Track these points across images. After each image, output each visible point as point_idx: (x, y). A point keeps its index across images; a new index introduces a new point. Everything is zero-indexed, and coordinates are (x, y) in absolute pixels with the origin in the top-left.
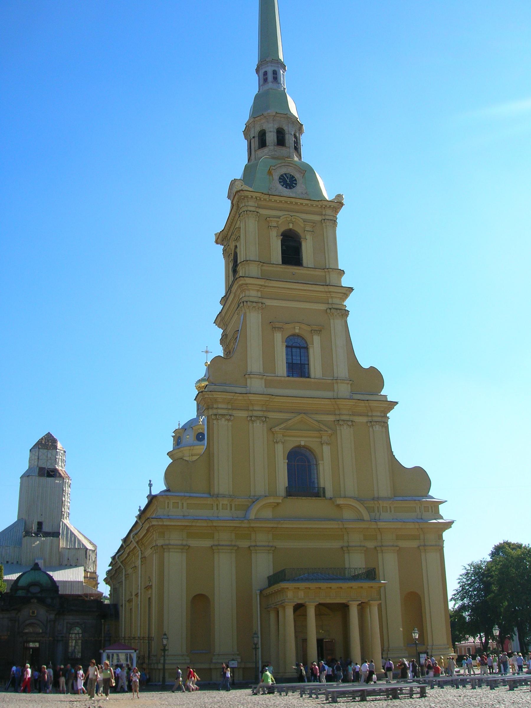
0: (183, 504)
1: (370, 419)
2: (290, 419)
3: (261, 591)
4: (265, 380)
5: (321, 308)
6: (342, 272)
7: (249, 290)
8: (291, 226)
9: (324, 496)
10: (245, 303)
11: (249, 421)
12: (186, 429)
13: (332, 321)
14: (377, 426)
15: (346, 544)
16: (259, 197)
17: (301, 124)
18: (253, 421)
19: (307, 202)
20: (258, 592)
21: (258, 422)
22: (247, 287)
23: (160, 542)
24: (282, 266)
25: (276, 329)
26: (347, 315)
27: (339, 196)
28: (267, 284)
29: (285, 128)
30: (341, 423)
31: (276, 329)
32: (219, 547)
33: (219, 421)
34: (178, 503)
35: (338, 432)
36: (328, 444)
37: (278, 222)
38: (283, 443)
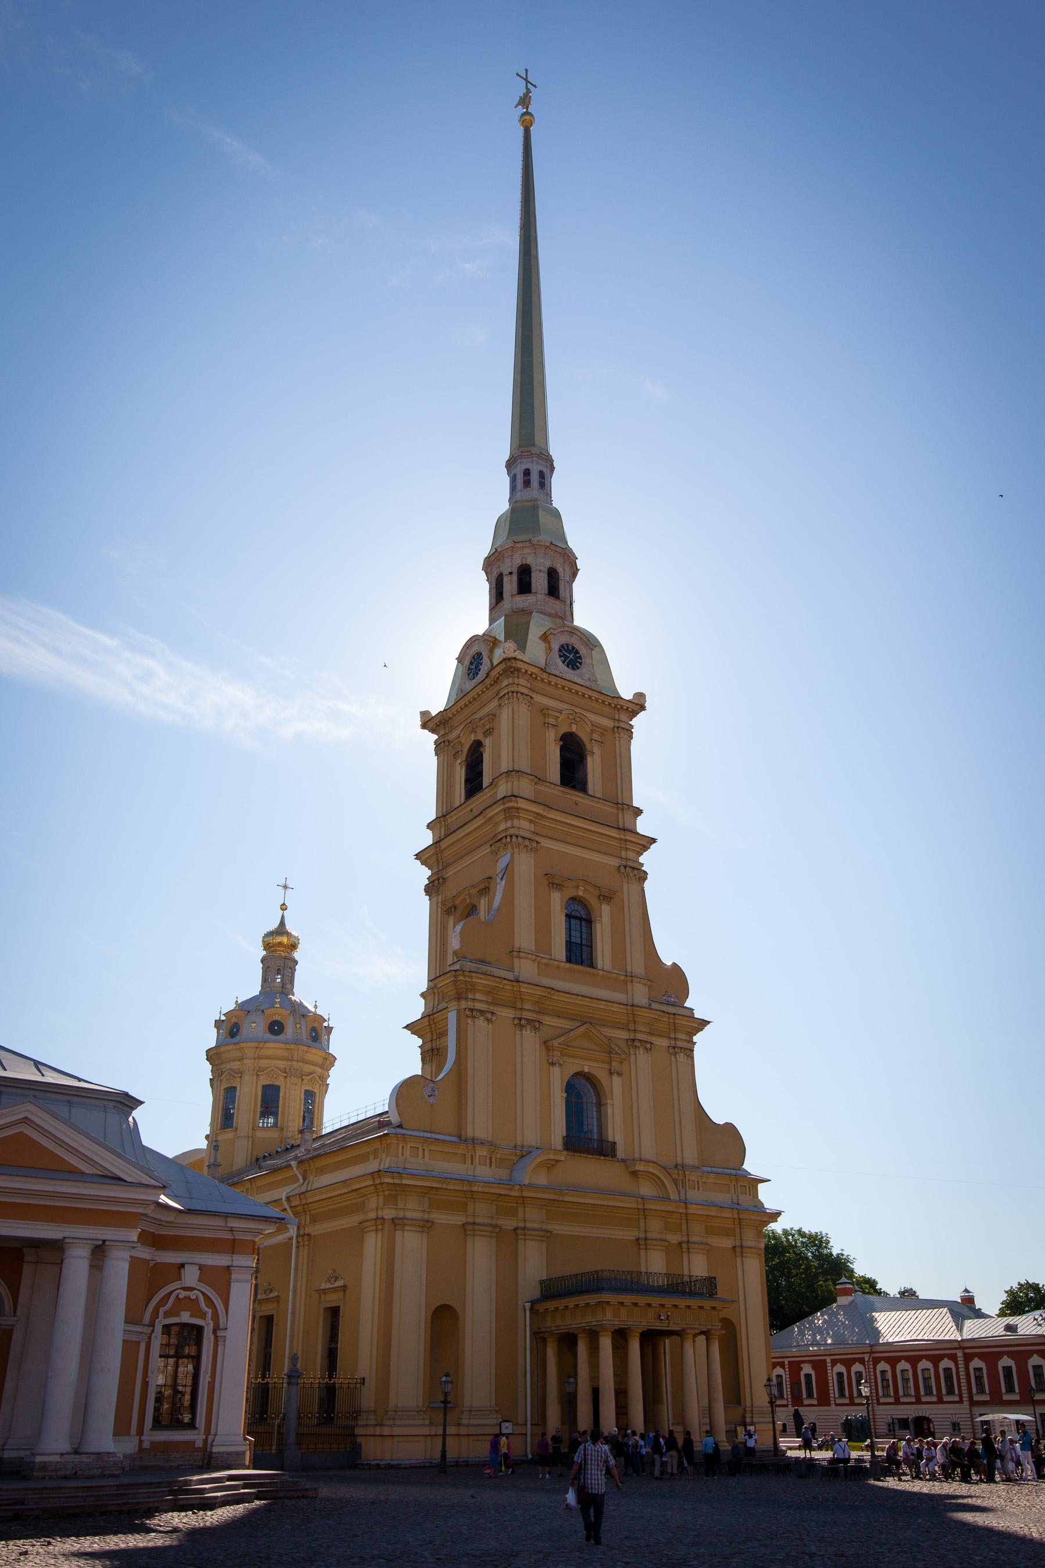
0: (424, 1149)
1: (673, 1042)
2: (572, 1030)
3: (532, 1308)
4: (539, 963)
5: (612, 863)
6: (638, 812)
7: (519, 818)
8: (574, 729)
9: (615, 1156)
10: (514, 838)
11: (515, 1025)
12: (249, 1012)
13: (625, 885)
14: (682, 1055)
15: (642, 1235)
16: (535, 674)
17: (577, 568)
18: (522, 1026)
19: (595, 695)
20: (528, 1305)
21: (528, 1027)
22: (518, 813)
23: (389, 1214)
24: (562, 789)
25: (555, 886)
26: (646, 879)
27: (640, 696)
28: (545, 814)
29: (560, 570)
30: (638, 1044)
31: (555, 886)
32: (477, 1227)
33: (476, 1020)
34: (418, 1148)
35: (632, 1057)
36: (620, 1074)
37: (559, 718)
38: (560, 1065)
